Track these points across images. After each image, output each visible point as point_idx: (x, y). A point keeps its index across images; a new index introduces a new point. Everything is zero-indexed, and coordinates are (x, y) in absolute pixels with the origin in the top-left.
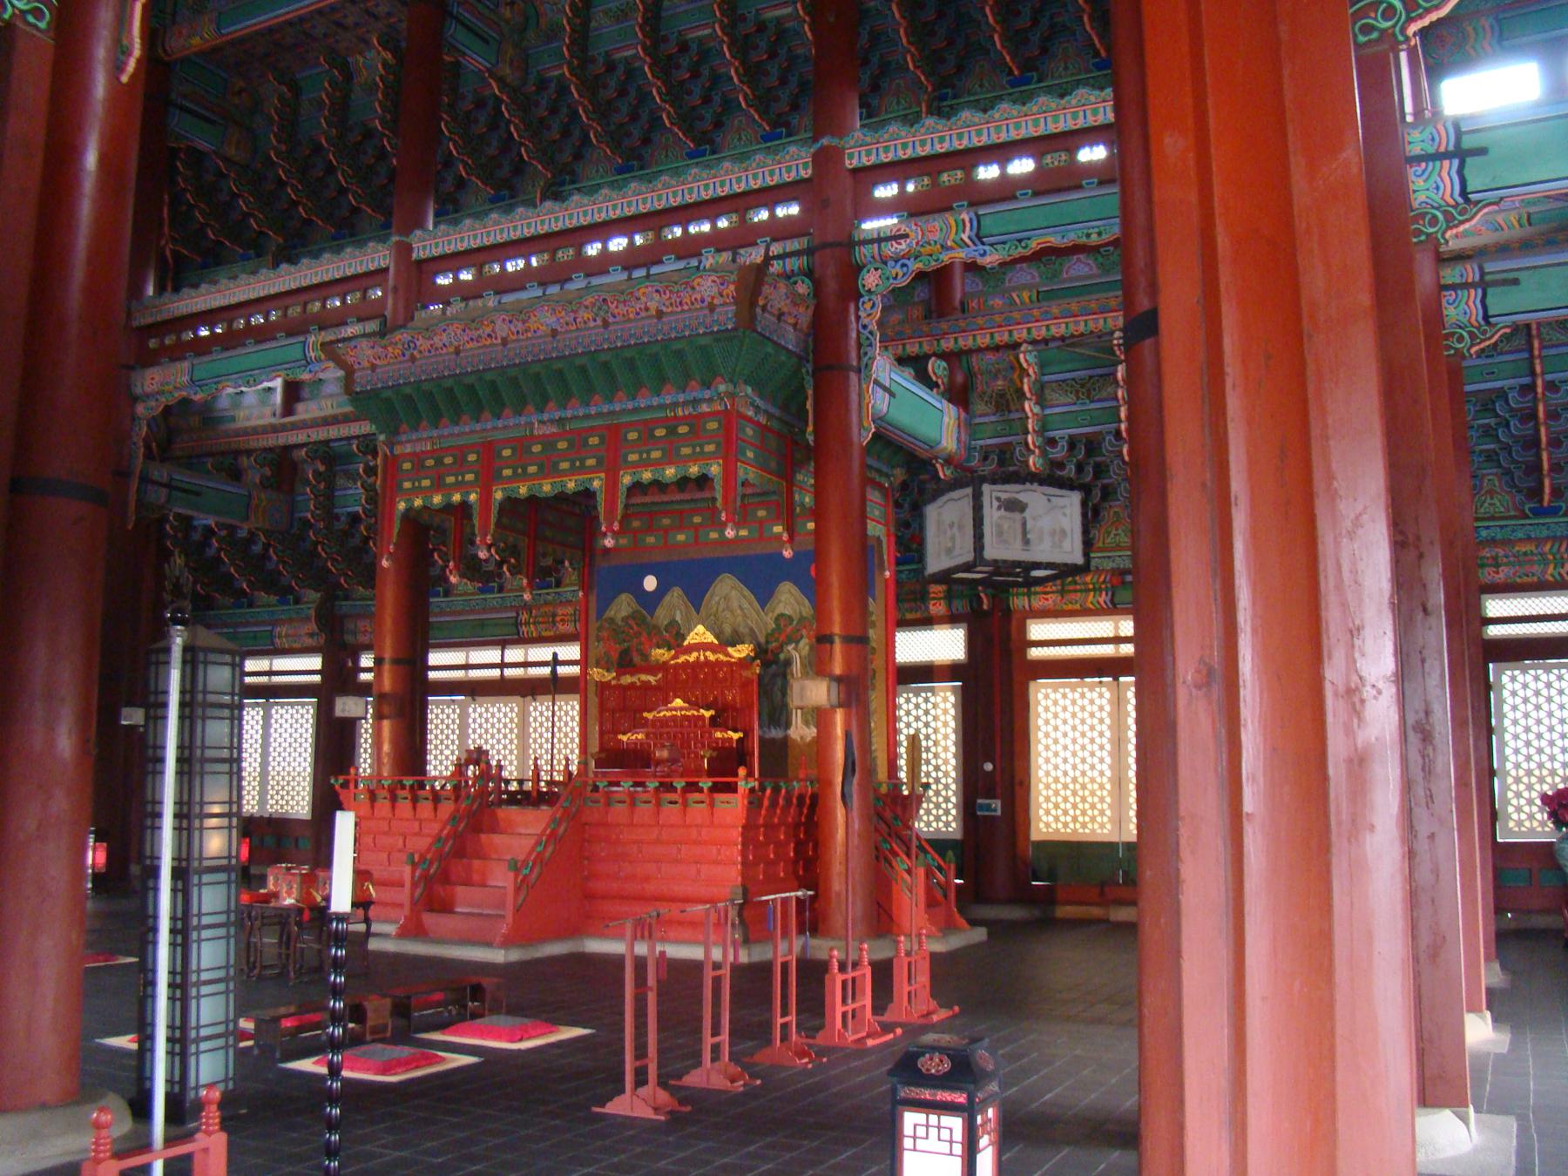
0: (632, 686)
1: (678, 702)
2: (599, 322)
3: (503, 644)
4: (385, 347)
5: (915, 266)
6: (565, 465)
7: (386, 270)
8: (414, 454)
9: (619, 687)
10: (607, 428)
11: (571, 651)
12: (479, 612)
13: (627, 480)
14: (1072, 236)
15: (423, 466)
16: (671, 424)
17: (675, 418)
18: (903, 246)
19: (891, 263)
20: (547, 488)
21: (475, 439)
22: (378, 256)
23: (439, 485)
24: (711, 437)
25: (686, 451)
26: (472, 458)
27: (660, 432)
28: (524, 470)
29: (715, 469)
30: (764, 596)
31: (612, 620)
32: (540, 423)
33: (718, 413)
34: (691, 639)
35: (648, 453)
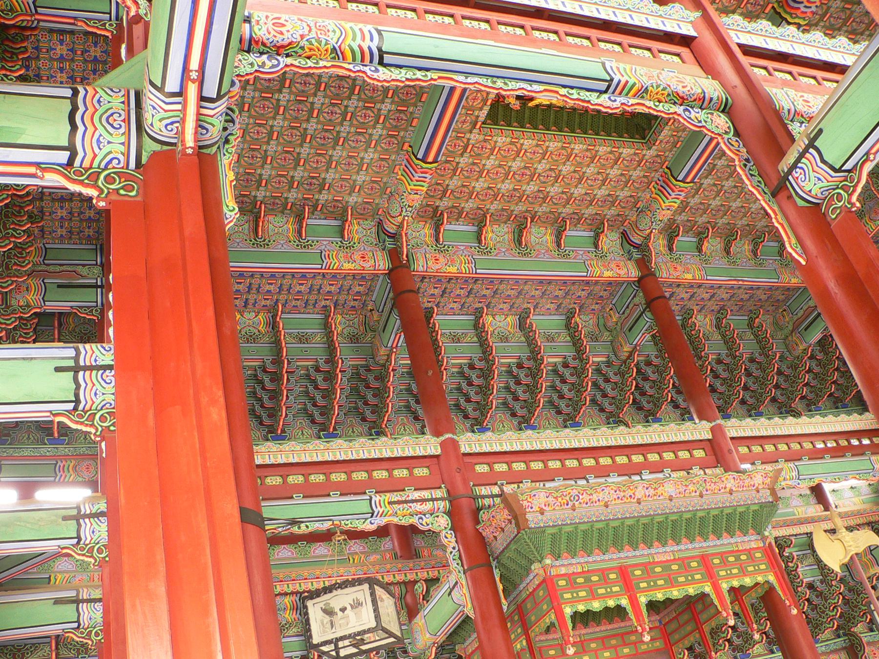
2: (698, 494)
4: (556, 498)
7: (437, 457)
13: (725, 586)
16: (736, 553)
17: (738, 551)
20: (676, 594)
23: (594, 596)
26: (613, 576)
27: (732, 559)
28: (655, 583)
29: (771, 578)
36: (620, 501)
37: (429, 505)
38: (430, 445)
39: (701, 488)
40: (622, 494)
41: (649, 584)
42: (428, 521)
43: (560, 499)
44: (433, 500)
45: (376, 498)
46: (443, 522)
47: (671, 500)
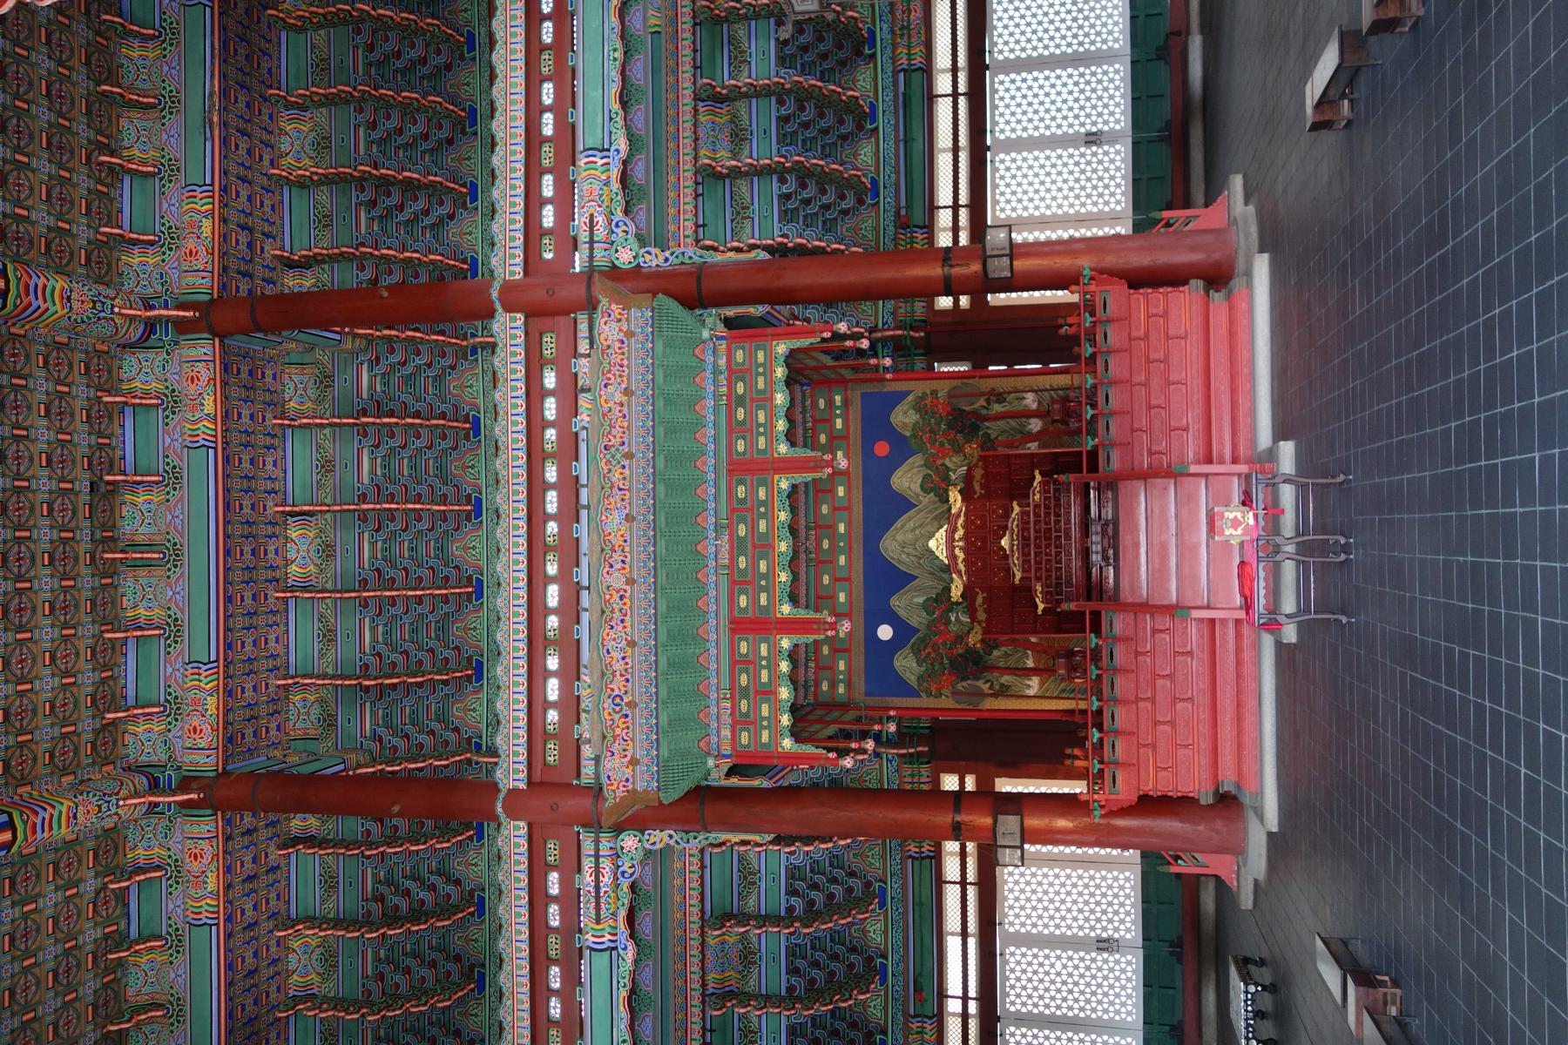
0: (986, 611)
1: (1004, 542)
2: (626, 463)
3: (940, 882)
4: (615, 737)
5: (619, 215)
6: (763, 526)
7: (530, 826)
8: (735, 724)
9: (988, 621)
10: (730, 472)
11: (952, 846)
12: (906, 907)
13: (783, 448)
14: (613, 73)
15: (747, 715)
16: (734, 401)
17: (729, 397)
18: (600, 219)
19: (613, 237)
21: (725, 640)
22: (513, 836)
23: (769, 693)
24: (751, 357)
25: (761, 384)
26: (744, 648)
27: (740, 414)
28: (763, 577)
29: (782, 348)
30: (903, 505)
31: (920, 678)
32: (716, 548)
33: (729, 350)
34: (942, 555)
35: (759, 425)
36: (628, 618)
37: (606, 864)
38: (513, 836)
39: (618, 456)
40: (617, 614)
41: (762, 589)
42: (628, 864)
43: (618, 731)
44: (597, 857)
45: (589, 939)
46: (629, 841)
47: (634, 519)
